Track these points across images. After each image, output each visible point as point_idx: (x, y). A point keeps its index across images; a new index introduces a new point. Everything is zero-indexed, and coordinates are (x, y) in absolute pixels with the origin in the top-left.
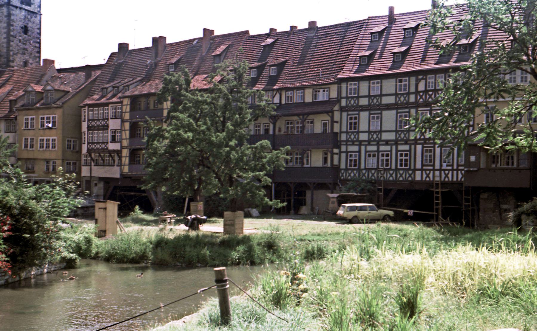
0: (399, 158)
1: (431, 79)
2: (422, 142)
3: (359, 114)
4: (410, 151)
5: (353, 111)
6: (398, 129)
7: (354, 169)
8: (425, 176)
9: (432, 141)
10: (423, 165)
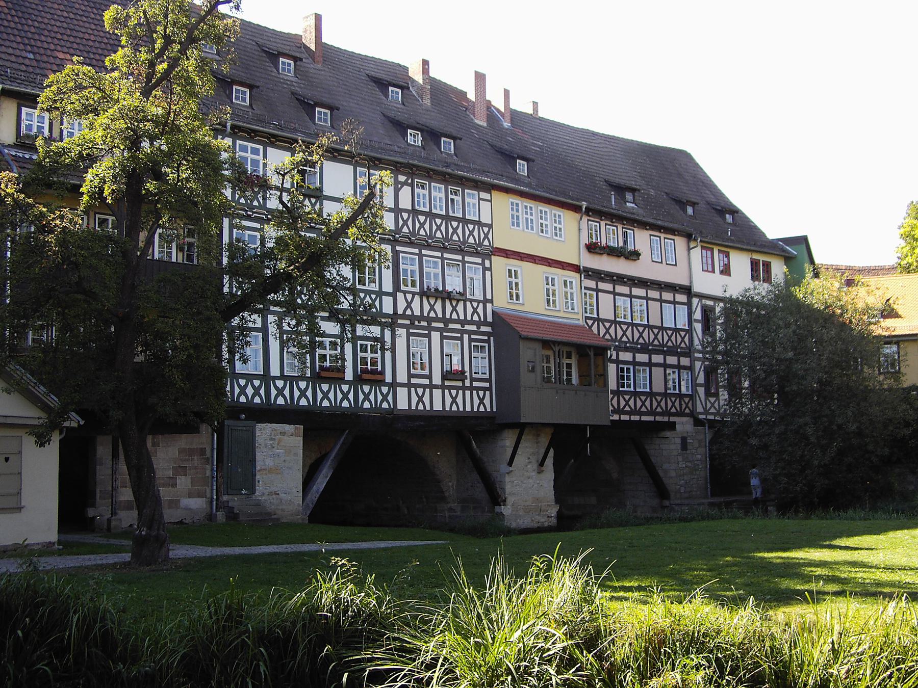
2: (408, 322)
5: (248, 218)
7: (256, 377)
8: (415, 399)
9: (424, 324)
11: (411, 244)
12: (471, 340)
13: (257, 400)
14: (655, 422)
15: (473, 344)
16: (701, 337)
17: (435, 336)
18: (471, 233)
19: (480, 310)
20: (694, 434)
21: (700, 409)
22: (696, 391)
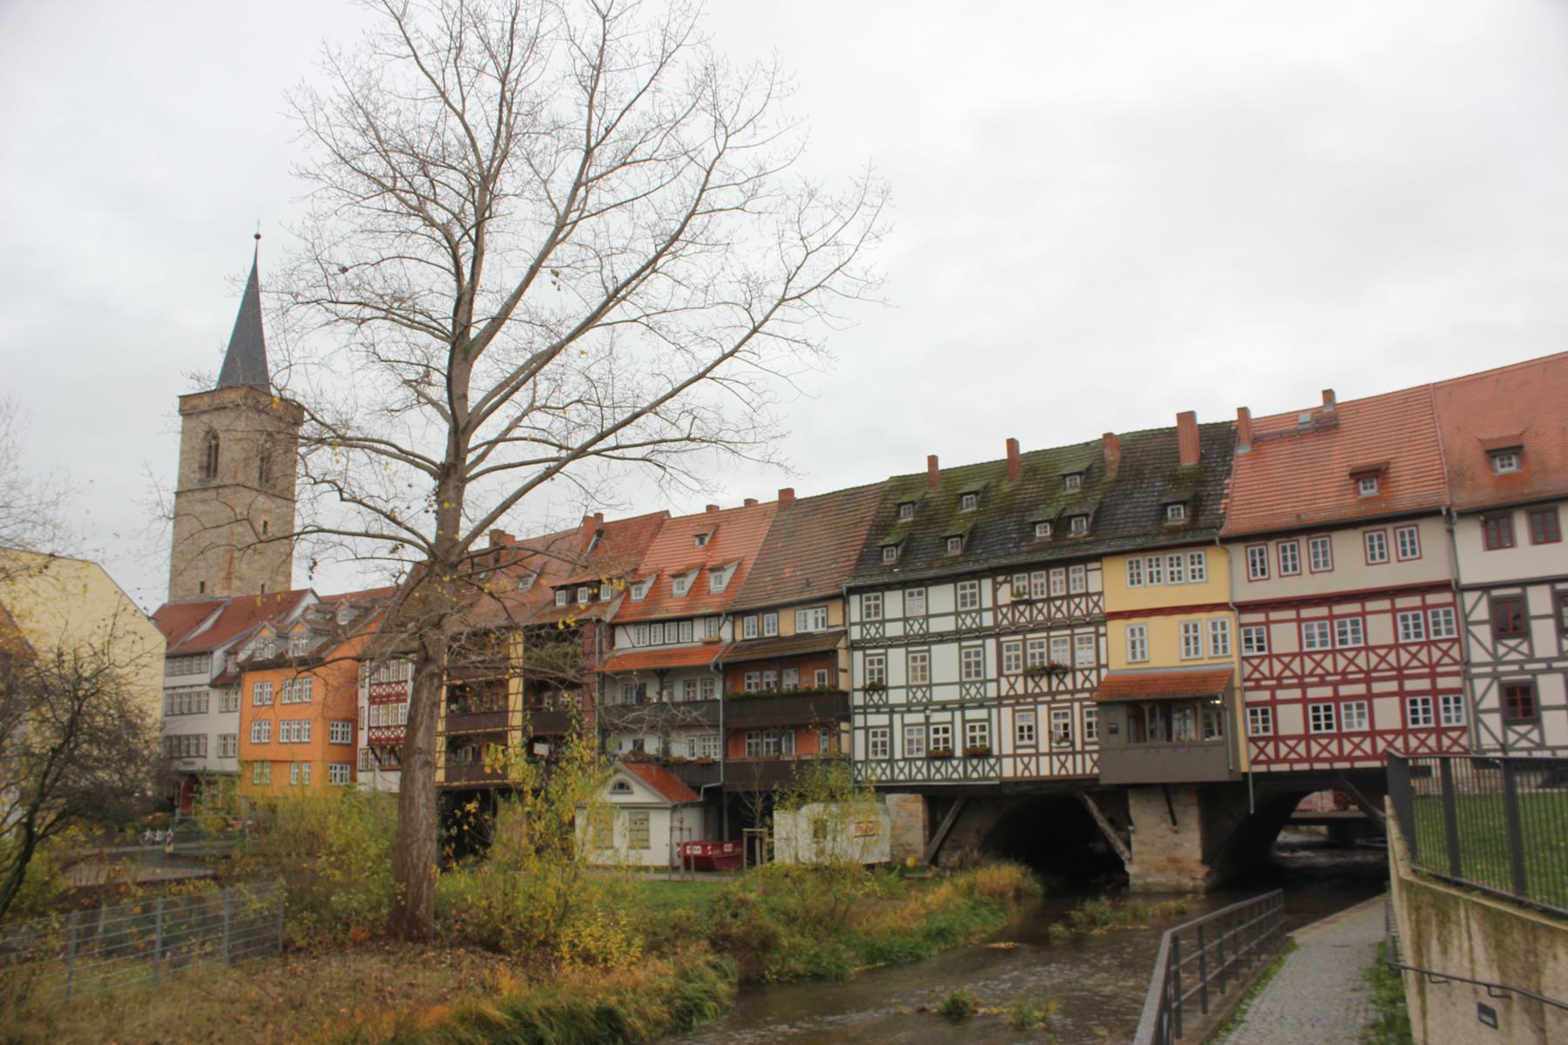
0: (969, 734)
1: (1021, 581)
2: (1013, 701)
3: (886, 654)
4: (989, 720)
5: (875, 647)
6: (964, 679)
7: (884, 761)
10: (1016, 747)
11: (1015, 633)
12: (1082, 707)
13: (884, 778)
15: (1085, 710)
16: (1490, 647)
17: (1043, 709)
18: (1078, 606)
19: (1093, 677)
21: (1487, 741)
22: (1478, 721)
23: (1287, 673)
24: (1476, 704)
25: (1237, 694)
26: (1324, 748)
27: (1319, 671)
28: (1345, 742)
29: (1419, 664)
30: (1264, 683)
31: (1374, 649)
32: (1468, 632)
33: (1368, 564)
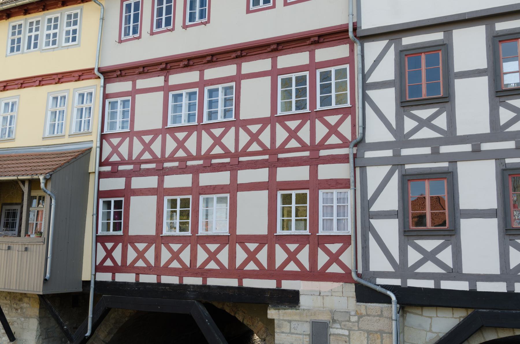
14: (240, 289)
16: (392, 120)
20: (354, 319)
22: (368, 228)
23: (147, 156)
24: (367, 203)
25: (93, 180)
26: (175, 256)
27: (181, 153)
28: (200, 249)
29: (297, 145)
30: (121, 168)
31: (244, 124)
32: (365, 98)
33: (248, 11)
